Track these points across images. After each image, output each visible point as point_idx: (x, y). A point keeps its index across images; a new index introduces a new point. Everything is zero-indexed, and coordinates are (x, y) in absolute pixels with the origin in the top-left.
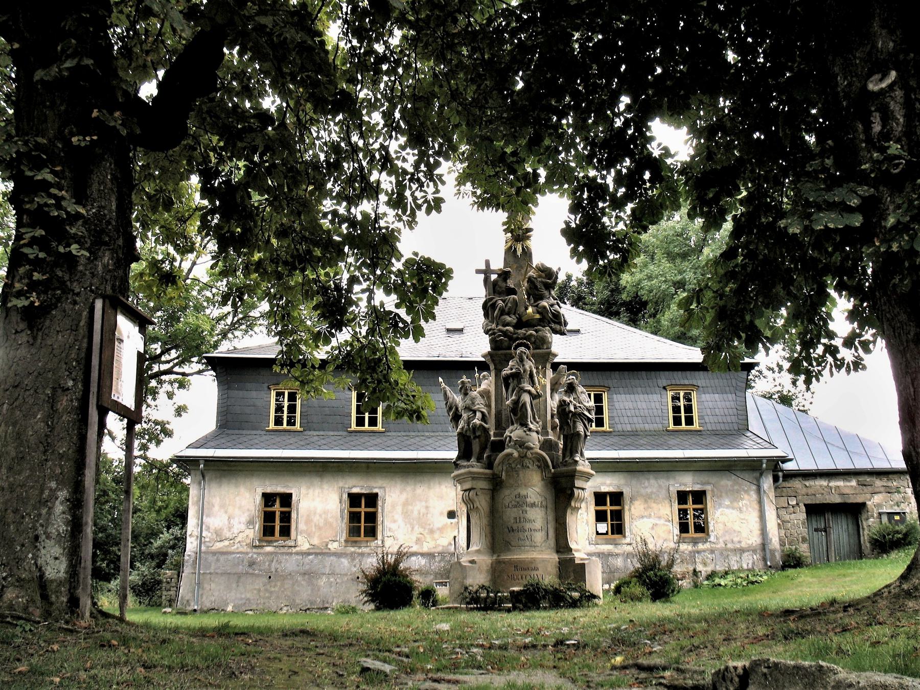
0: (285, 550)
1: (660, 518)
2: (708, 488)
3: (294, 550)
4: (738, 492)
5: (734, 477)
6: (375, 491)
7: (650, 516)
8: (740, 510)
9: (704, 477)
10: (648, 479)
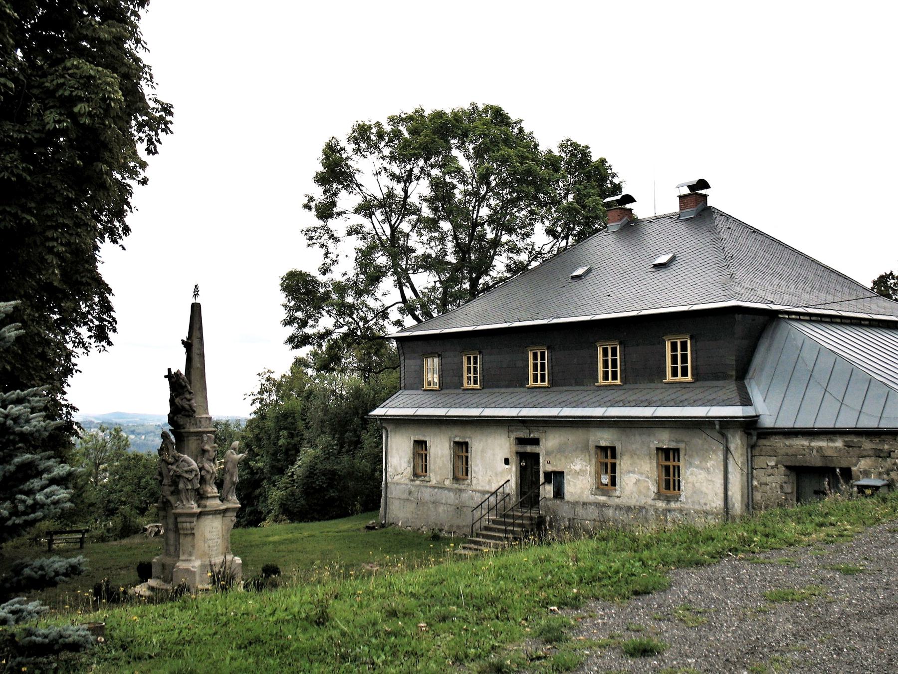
0: (425, 484)
1: (642, 474)
2: (681, 446)
3: (429, 484)
4: (707, 451)
5: (704, 435)
6: (467, 440)
7: (634, 472)
10: (634, 435)
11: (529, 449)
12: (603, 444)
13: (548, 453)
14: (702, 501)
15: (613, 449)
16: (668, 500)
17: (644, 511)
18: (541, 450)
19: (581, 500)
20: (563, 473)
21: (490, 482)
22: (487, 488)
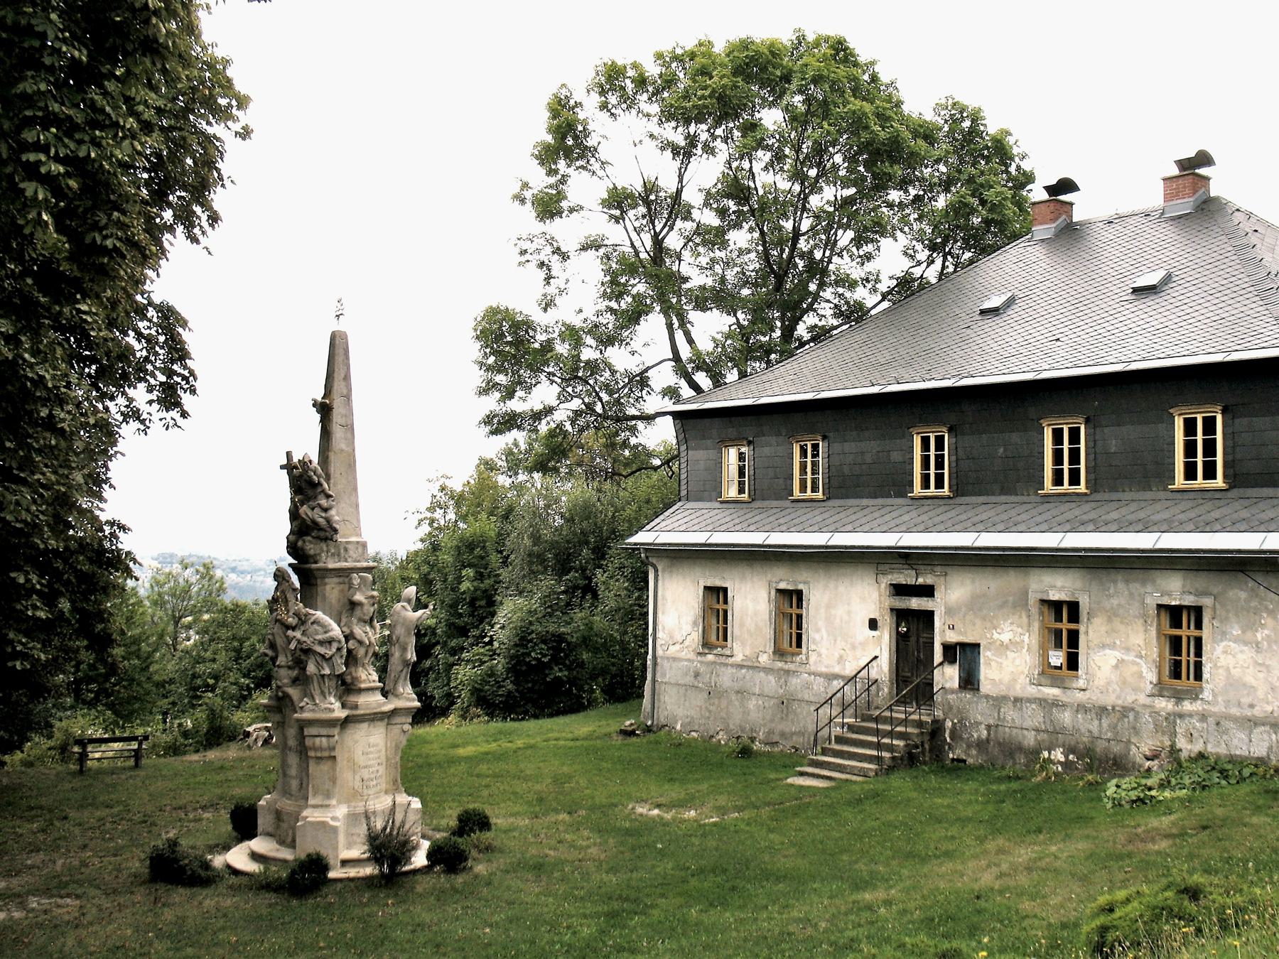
0: (723, 660)
1: (1128, 649)
2: (1206, 602)
3: (731, 660)
4: (1257, 612)
5: (1251, 584)
6: (800, 587)
7: (1113, 647)
8: (1257, 647)
9: (1201, 581)
10: (1115, 582)
11: (915, 603)
12: (1055, 596)
13: (949, 611)
14: (1246, 700)
15: (1074, 608)
16: (1178, 697)
17: (1131, 716)
18: (936, 605)
19: (1012, 694)
20: (978, 645)
21: (841, 660)
22: (837, 669)
